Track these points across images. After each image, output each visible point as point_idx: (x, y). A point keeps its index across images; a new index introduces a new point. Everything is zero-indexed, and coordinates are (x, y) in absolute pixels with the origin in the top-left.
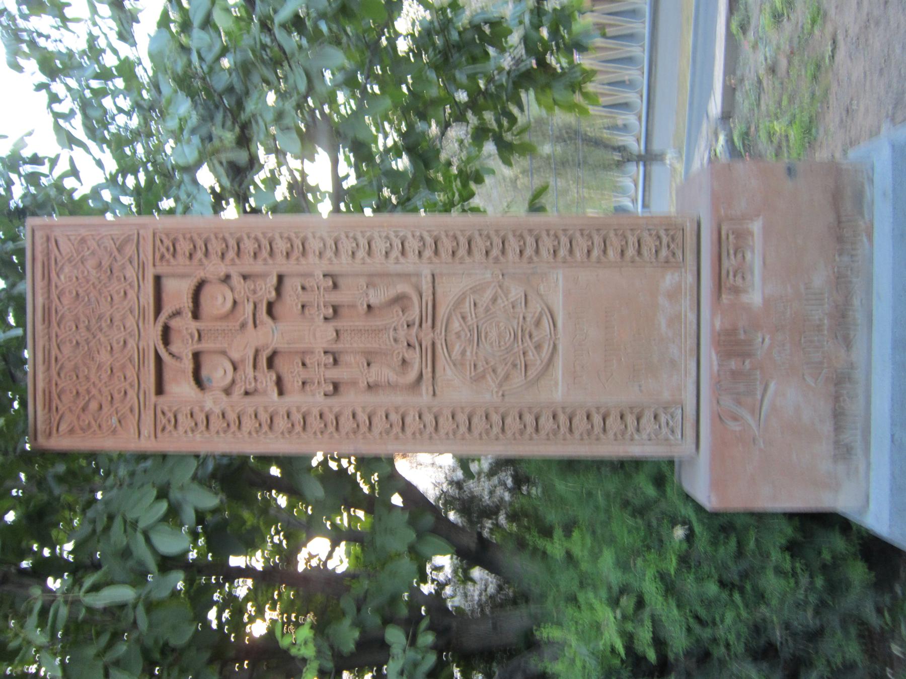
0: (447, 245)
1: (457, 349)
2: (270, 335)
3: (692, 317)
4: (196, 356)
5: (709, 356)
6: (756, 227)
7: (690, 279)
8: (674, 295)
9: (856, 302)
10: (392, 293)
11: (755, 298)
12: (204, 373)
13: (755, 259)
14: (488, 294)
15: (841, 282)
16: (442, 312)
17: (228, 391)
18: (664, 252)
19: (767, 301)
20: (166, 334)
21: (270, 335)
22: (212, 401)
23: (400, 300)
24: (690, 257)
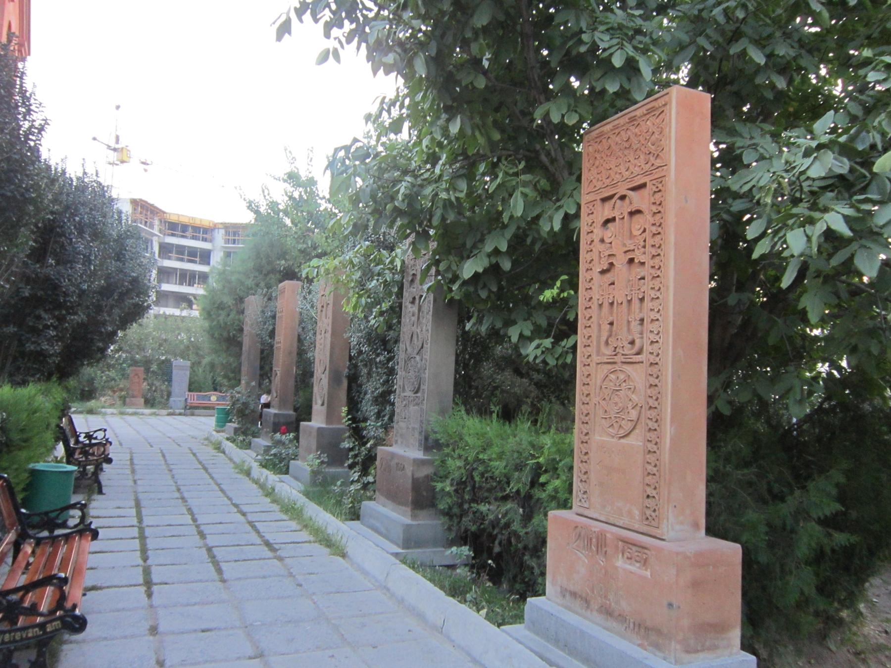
0: (654, 370)
1: (612, 376)
2: (620, 262)
3: (621, 524)
4: (614, 219)
5: (597, 527)
6: (648, 573)
7: (636, 526)
8: (630, 513)
9: (615, 624)
10: (637, 336)
11: (620, 562)
12: (610, 225)
13: (634, 568)
14: (634, 397)
15: (621, 618)
16: (627, 368)
17: (602, 241)
18: (648, 512)
19: (616, 568)
20: (623, 198)
21: (620, 262)
22: (598, 232)
23: (632, 343)
24: (645, 529)
